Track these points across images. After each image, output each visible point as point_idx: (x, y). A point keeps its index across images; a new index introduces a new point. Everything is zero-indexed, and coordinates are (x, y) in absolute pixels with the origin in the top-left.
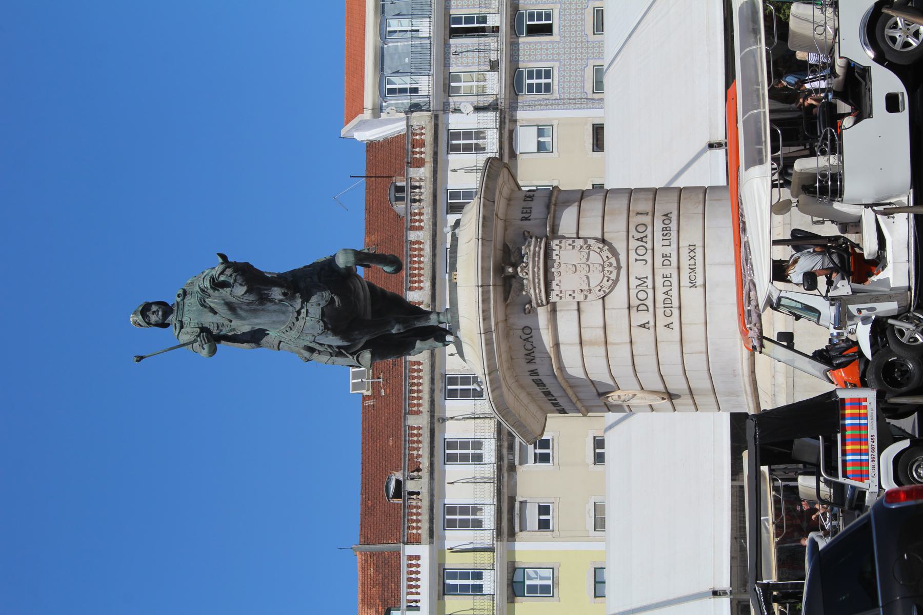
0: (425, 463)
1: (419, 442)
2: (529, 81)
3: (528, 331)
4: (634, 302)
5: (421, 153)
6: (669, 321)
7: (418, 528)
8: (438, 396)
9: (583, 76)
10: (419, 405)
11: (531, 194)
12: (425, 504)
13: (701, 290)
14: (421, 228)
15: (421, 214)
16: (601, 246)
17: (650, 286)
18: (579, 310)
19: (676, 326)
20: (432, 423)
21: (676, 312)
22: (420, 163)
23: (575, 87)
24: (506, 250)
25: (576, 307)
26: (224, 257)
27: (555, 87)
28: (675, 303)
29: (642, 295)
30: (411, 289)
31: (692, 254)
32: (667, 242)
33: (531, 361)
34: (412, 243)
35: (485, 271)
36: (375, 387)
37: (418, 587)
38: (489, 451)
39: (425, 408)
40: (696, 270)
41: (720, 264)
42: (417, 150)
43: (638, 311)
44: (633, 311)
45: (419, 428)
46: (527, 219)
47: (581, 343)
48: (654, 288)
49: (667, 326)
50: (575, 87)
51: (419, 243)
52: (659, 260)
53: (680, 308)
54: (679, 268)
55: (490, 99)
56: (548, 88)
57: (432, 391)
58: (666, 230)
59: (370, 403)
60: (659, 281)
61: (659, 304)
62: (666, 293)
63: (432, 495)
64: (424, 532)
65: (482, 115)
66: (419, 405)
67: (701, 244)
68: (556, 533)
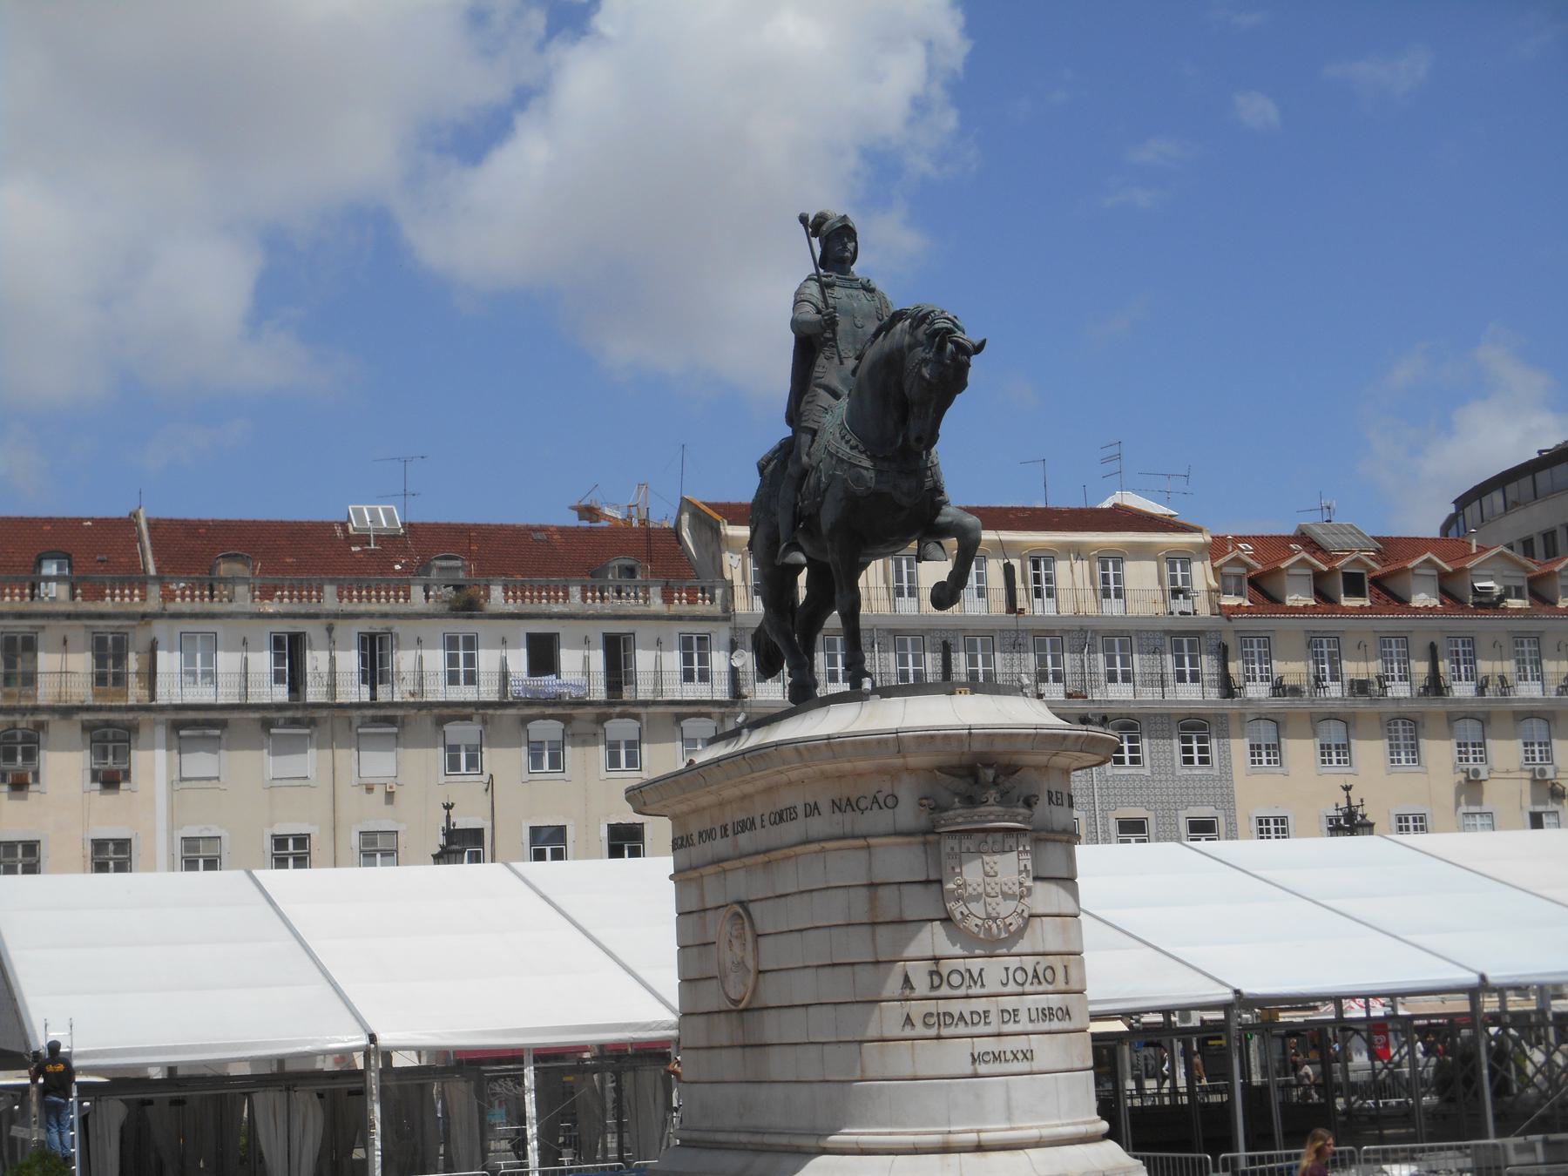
0: (270, 607)
3: (890, 802)
4: (945, 966)
5: (680, 599)
6: (918, 1021)
10: (350, 598)
11: (1066, 803)
12: (216, 607)
13: (969, 1070)
14: (584, 599)
15: (602, 598)
16: (1026, 914)
17: (972, 992)
18: (927, 882)
19: (908, 1032)
20: (328, 616)
21: (933, 1032)
22: (667, 599)
24: (1011, 769)
25: (932, 877)
26: (979, 348)
28: (945, 1032)
29: (956, 980)
30: (506, 590)
31: (1020, 1056)
32: (1034, 1016)
33: (836, 805)
35: (991, 738)
36: (363, 539)
39: (346, 606)
40: (997, 1064)
41: (1008, 1099)
43: (931, 973)
44: (929, 965)
46: (1050, 799)
47: (872, 885)
48: (968, 997)
49: (908, 1020)
52: (1009, 1003)
53: (939, 1038)
54: (999, 1035)
55: (745, 691)
57: (371, 615)
58: (1048, 1014)
59: (339, 532)
60: (980, 1005)
61: (943, 1006)
62: (962, 1017)
63: (230, 615)
65: (725, 678)
67: (1035, 1069)
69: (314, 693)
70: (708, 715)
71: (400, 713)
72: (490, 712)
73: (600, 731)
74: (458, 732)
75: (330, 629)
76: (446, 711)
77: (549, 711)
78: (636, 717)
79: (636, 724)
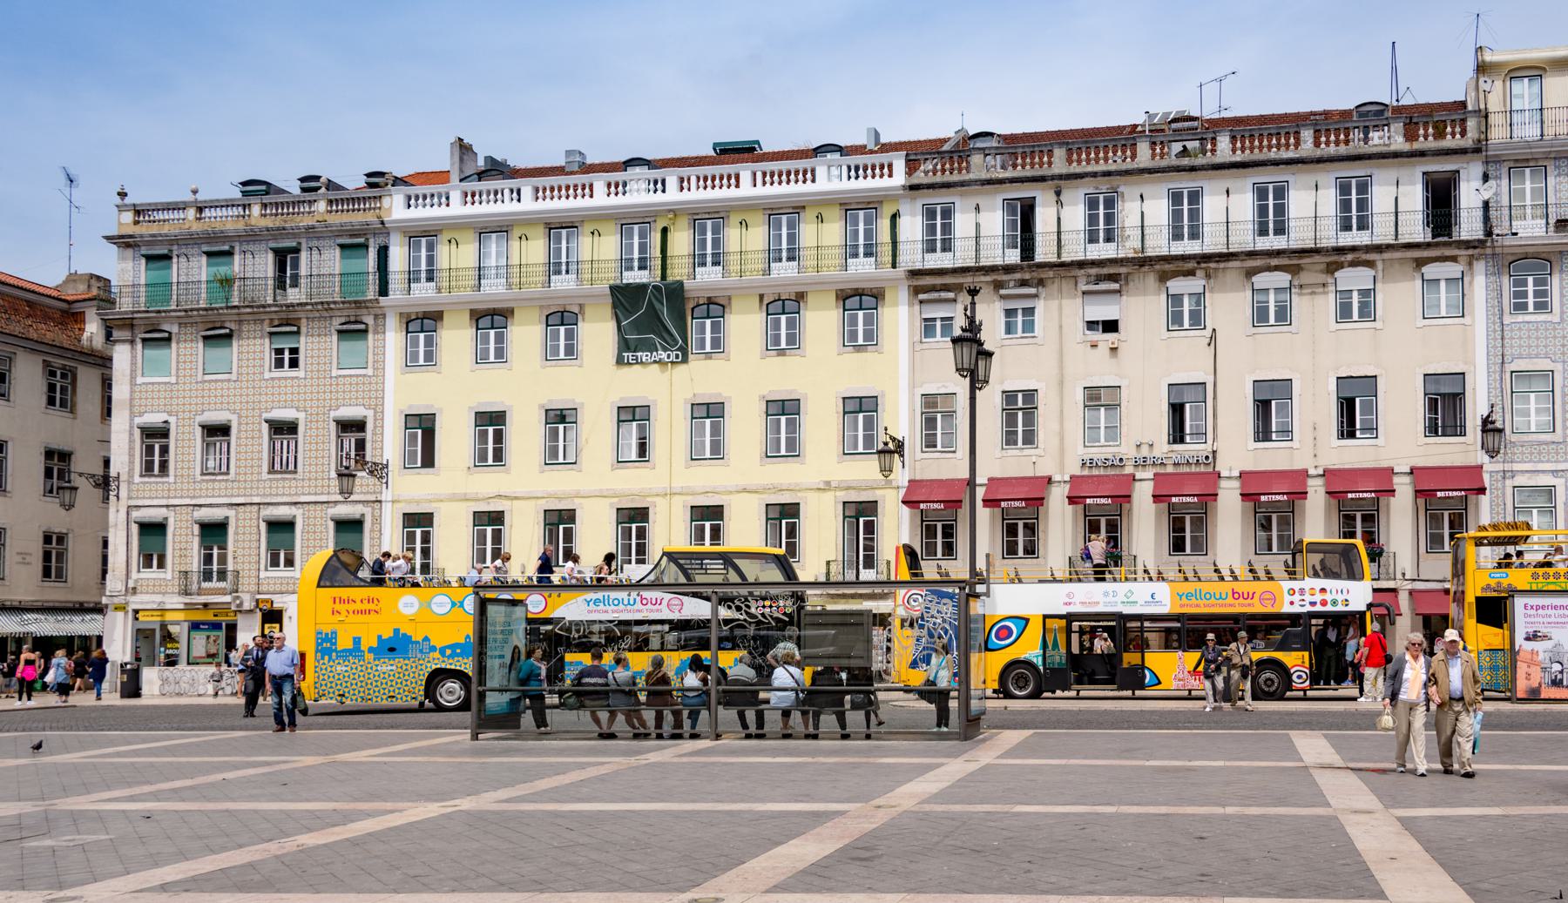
1: (1032, 165)
2: (1530, 279)
7: (1453, 134)
8: (1087, 187)
9: (1537, 356)
10: (1079, 161)
14: (1317, 144)
20: (1053, 178)
23: (1520, 346)
27: (1520, 318)
30: (1233, 139)
34: (1297, 133)
37: (788, 182)
38: (1187, 247)
39: (1075, 168)
42: (1431, 130)
45: (1050, 164)
50: (1520, 346)
51: (1297, 144)
56: (1521, 307)
57: (1094, 175)
63: (962, 184)
64: (919, 178)
66: (1079, 161)
68: (918, 347)
69: (1044, 251)
70: (1454, 259)
71: (1123, 270)
72: (1213, 265)
73: (1331, 280)
74: (1353, 279)
75: (1058, 193)
76: (1167, 267)
77: (1274, 262)
78: (1370, 264)
79: (1371, 272)
